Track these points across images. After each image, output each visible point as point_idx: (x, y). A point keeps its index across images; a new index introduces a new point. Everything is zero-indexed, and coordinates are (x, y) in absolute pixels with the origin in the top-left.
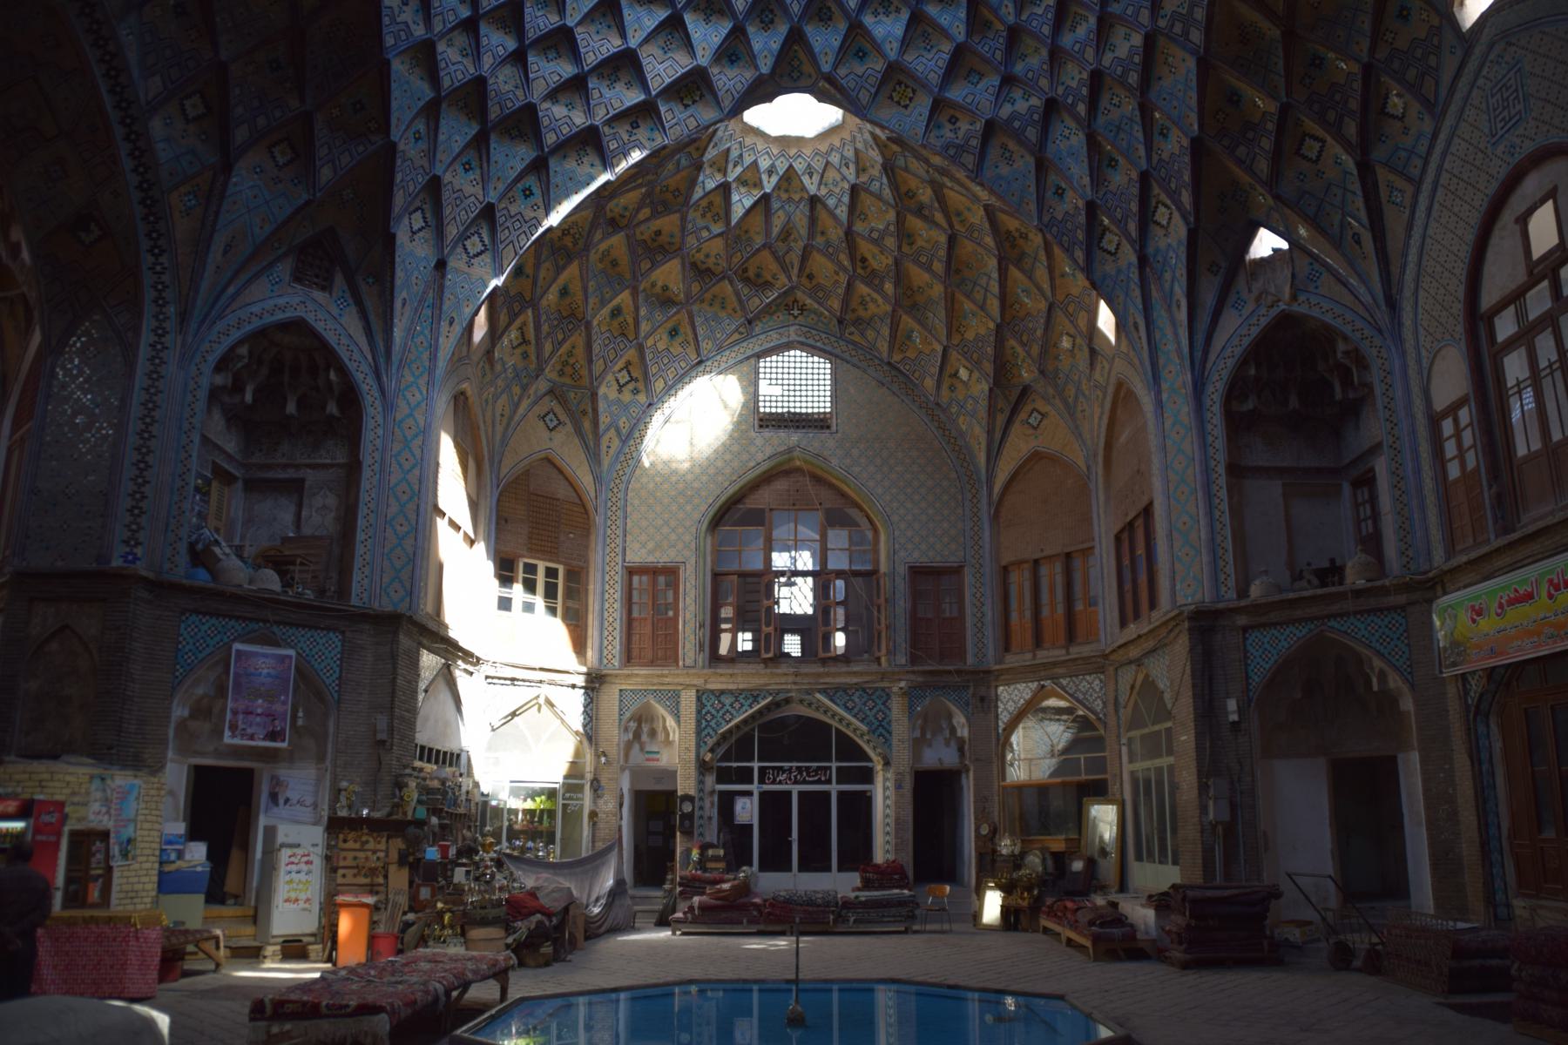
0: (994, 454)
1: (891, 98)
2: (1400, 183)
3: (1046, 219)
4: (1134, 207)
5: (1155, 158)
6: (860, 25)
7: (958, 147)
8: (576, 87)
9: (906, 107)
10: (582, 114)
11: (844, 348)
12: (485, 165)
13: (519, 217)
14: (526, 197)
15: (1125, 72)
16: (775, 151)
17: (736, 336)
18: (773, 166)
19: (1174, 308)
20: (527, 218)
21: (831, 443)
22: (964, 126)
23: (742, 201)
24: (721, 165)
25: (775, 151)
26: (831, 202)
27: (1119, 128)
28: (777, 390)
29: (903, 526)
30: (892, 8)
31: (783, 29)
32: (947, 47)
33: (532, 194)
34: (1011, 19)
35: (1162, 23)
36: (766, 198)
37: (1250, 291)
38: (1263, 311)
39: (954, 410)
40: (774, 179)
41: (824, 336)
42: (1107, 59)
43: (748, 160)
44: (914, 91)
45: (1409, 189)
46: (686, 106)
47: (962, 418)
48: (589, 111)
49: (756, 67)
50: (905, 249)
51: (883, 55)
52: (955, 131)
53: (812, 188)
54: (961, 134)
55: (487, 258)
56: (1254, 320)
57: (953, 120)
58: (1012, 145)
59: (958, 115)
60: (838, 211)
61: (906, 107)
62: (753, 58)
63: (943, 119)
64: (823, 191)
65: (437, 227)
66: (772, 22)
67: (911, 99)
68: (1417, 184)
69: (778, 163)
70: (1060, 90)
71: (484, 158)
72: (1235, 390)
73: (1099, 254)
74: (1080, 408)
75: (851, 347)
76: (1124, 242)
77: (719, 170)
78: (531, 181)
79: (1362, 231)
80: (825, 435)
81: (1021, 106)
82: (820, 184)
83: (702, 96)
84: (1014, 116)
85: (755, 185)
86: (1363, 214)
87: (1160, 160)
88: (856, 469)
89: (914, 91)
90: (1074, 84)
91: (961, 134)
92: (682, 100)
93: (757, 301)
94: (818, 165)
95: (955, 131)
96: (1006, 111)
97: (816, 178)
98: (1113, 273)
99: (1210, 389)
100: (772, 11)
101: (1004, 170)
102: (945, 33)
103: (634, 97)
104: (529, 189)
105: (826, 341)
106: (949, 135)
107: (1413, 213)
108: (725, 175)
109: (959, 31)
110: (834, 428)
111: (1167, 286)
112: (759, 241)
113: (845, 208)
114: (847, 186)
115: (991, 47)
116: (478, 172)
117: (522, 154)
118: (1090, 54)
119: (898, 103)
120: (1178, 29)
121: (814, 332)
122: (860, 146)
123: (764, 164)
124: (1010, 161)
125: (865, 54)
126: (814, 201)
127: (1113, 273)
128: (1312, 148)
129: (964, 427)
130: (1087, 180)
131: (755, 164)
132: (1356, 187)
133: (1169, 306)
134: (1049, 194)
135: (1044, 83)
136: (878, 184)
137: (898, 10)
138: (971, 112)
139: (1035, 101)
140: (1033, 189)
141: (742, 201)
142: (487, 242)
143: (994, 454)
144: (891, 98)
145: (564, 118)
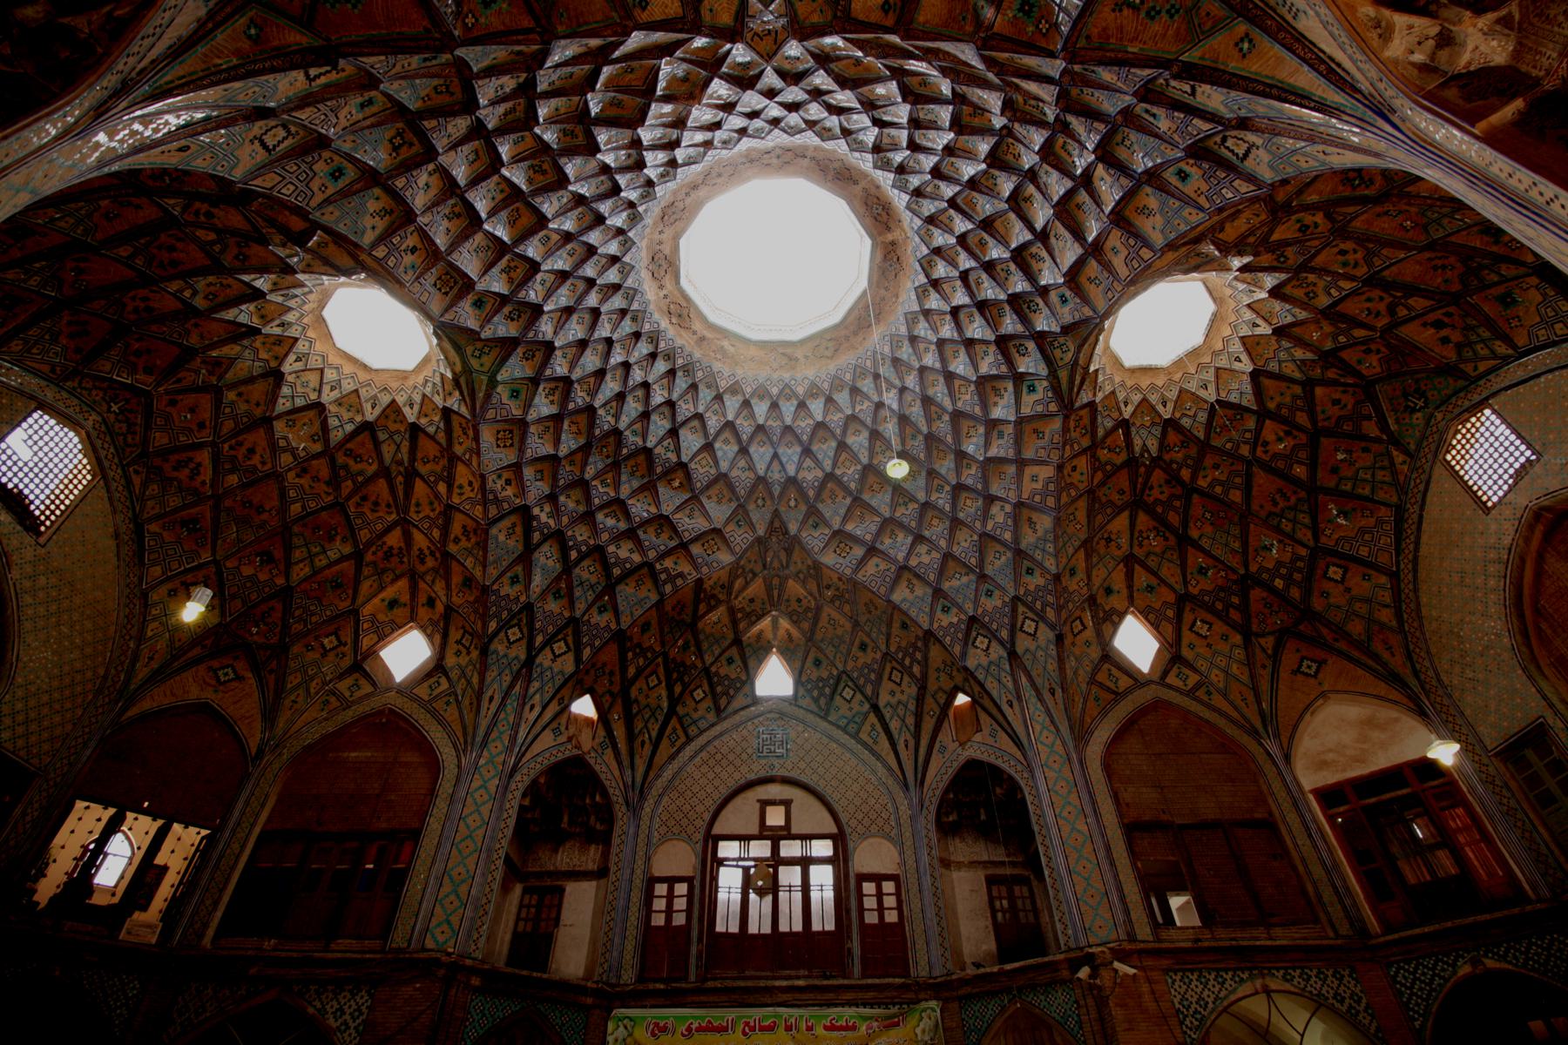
0: (156, 677)
1: (498, 432)
2: (680, 732)
3: (495, 587)
4: (550, 629)
5: (586, 618)
6: (538, 385)
7: (496, 497)
8: (450, 187)
9: (498, 446)
10: (423, 203)
11: (117, 477)
12: (368, 122)
13: (311, 174)
14: (332, 175)
15: (616, 564)
16: (305, 321)
17: (46, 368)
18: (290, 324)
19: (527, 708)
20: (311, 185)
21: (29, 554)
22: (509, 492)
23: (245, 314)
24: (276, 288)
25: (305, 321)
26: (285, 390)
27: (582, 583)
28: (25, 453)
29: (20, 693)
30: (551, 398)
31: (513, 333)
32: (552, 452)
33: (336, 179)
34: (587, 476)
35: (658, 566)
36: (257, 331)
37: (567, 728)
38: (569, 747)
39: (154, 612)
40: (278, 331)
41: (112, 450)
42: (612, 549)
43: (292, 303)
44: (512, 445)
45: (683, 739)
46: (435, 285)
47: (156, 624)
48: (428, 209)
49: (482, 327)
50: (291, 475)
51: (526, 412)
52: (503, 489)
53: (287, 368)
54: (504, 494)
55: (261, 155)
56: (562, 749)
57: (508, 482)
58: (519, 530)
59: (513, 483)
60: (281, 401)
61: (498, 446)
62: (487, 320)
63: (506, 475)
64: (290, 378)
65: (310, 95)
66: (512, 320)
67: (505, 446)
68: (689, 740)
69: (295, 327)
70: (570, 533)
71: (372, 120)
72: (532, 789)
73: (502, 634)
74: (293, 697)
75: (123, 481)
76: (524, 642)
77: (275, 284)
78: (351, 173)
79: (647, 741)
80: (28, 539)
81: (544, 518)
82: (296, 372)
83: (446, 294)
84: (537, 518)
85: (262, 317)
86: (654, 734)
87: (588, 621)
88: (28, 599)
89: (512, 445)
90: (580, 539)
91: (504, 494)
92: (440, 278)
93: (108, 367)
94: (314, 362)
95: (503, 489)
96: (536, 511)
97: (299, 366)
98: (501, 654)
99: (518, 777)
100: (519, 316)
101: (502, 538)
102: (557, 442)
103: (441, 241)
104: (342, 174)
105: (110, 456)
106: (499, 486)
107: (679, 751)
108: (272, 291)
109: (563, 451)
110: (42, 540)
111: (532, 690)
112: (194, 340)
113: (289, 405)
114: (313, 396)
115: (566, 473)
116: (360, 116)
117: (377, 156)
118: (605, 536)
119: (498, 439)
120: (663, 576)
121: (108, 439)
122: (363, 392)
123: (290, 317)
124: (509, 535)
125: (516, 397)
126: (277, 377)
127: (501, 654)
128: (653, 681)
129: (150, 634)
130: (537, 590)
131: (290, 309)
132: (661, 718)
133: (524, 704)
134: (509, 574)
135: (565, 520)
136: (337, 423)
137: (552, 402)
138: (522, 490)
139: (551, 522)
140: (505, 564)
141: (245, 314)
142: (282, 146)
143: (156, 677)
144: (498, 432)
145: (420, 190)
